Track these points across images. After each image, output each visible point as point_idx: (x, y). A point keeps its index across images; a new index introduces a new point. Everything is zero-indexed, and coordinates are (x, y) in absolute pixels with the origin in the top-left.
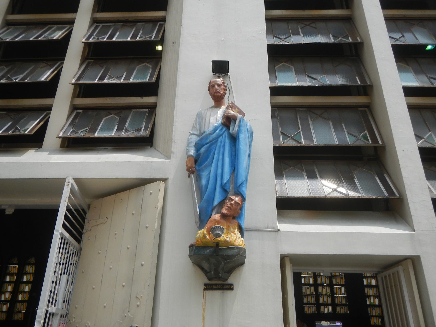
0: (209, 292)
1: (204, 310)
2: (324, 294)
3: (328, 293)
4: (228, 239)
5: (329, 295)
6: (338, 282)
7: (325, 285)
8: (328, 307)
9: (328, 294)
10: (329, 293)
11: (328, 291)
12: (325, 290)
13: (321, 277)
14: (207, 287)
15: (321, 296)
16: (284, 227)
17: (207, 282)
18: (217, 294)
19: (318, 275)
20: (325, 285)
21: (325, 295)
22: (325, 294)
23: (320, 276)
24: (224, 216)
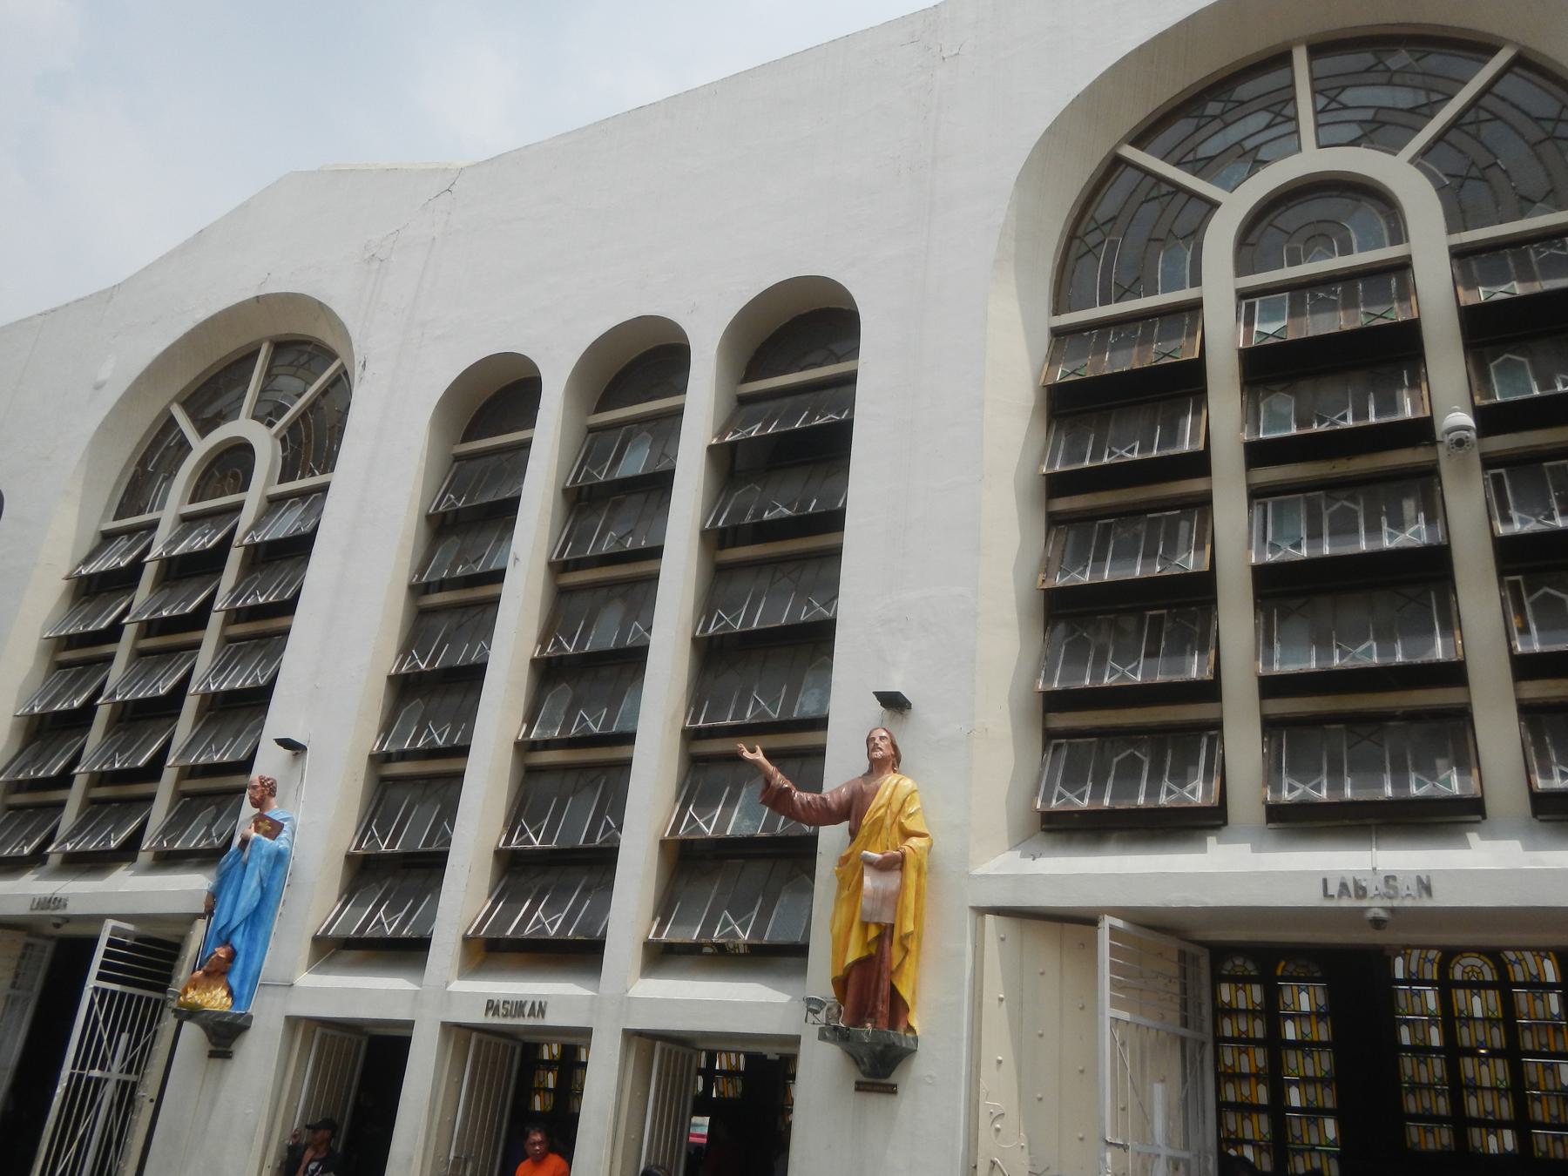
0: (212, 1060)
1: (203, 1081)
2: (1486, 1083)
3: (1502, 1083)
4: (199, 1002)
5: (1507, 1090)
6: (1544, 1041)
7: (1483, 1051)
8: (1499, 1132)
9: (1502, 1086)
10: (1504, 1083)
11: (1501, 1076)
12: (1494, 1073)
13: (1471, 1023)
14: (213, 1055)
15: (1472, 1090)
16: (306, 980)
17: (213, 1048)
18: (219, 1061)
19: (1463, 1015)
20: (1483, 1051)
21: (1493, 1089)
22: (1489, 1085)
23: (1471, 1018)
24: (207, 974)
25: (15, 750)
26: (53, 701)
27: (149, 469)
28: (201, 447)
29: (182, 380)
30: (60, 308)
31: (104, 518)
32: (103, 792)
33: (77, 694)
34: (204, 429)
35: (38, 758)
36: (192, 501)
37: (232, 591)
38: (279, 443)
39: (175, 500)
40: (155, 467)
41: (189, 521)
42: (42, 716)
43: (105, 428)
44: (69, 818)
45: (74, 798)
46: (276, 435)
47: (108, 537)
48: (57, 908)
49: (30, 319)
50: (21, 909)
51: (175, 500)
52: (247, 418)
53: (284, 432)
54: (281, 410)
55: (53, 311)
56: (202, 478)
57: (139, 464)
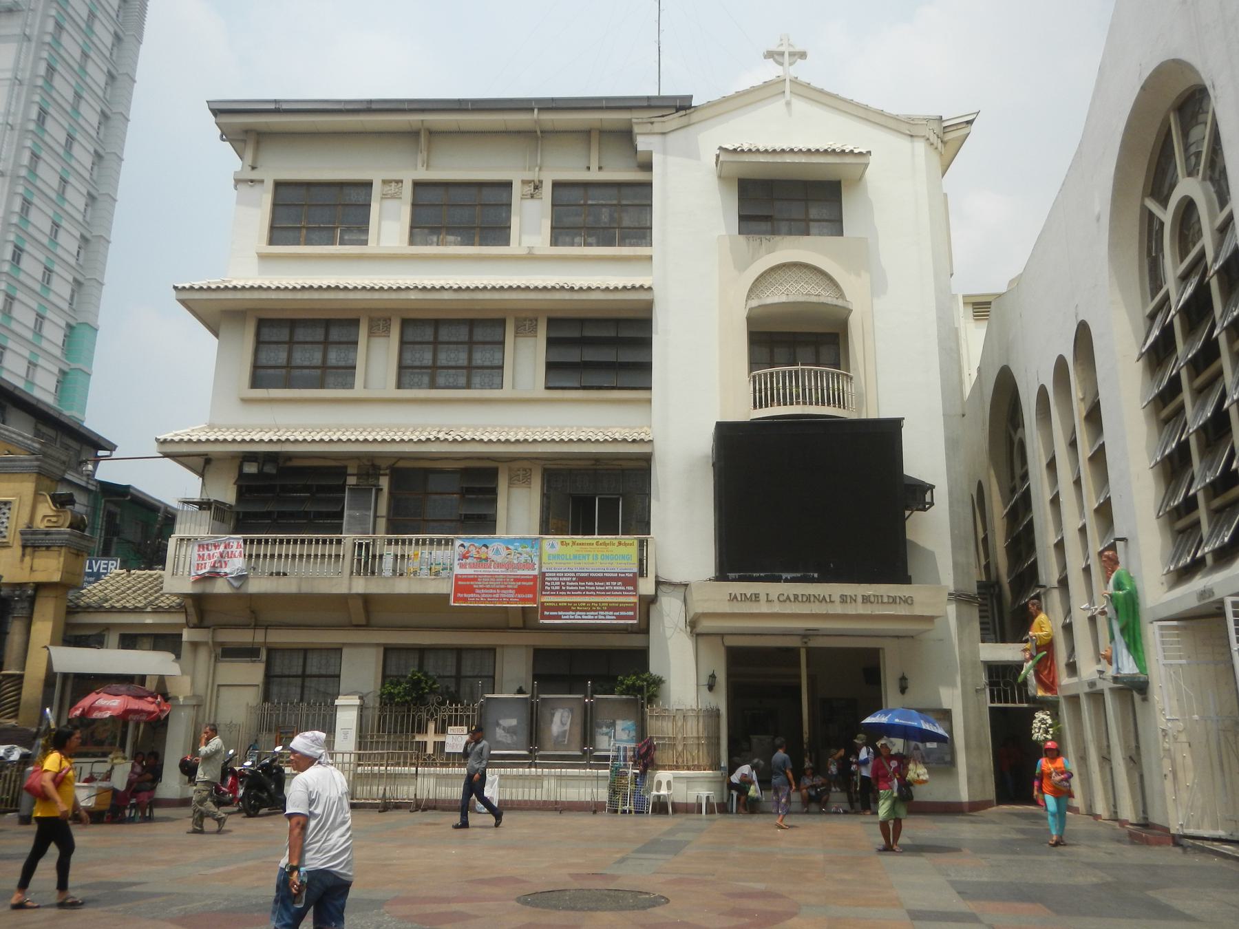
25: (1164, 492)
26: (1164, 451)
27: (1154, 255)
28: (1167, 217)
29: (1139, 181)
30: (1065, 180)
31: (1145, 305)
32: (1217, 503)
33: (1174, 440)
34: (1164, 203)
35: (1174, 494)
36: (1182, 261)
37: (1221, 316)
38: (1209, 184)
39: (1172, 269)
40: (1156, 252)
41: (1184, 278)
42: (1163, 460)
43: (1114, 245)
44: (1205, 528)
45: (1202, 513)
46: (1204, 179)
47: (1152, 317)
48: (1210, 597)
49: (1057, 197)
50: (1192, 603)
51: (1172, 269)
52: (1183, 178)
53: (1208, 172)
54: (1198, 154)
55: (1063, 184)
56: (1180, 242)
57: (1148, 256)
